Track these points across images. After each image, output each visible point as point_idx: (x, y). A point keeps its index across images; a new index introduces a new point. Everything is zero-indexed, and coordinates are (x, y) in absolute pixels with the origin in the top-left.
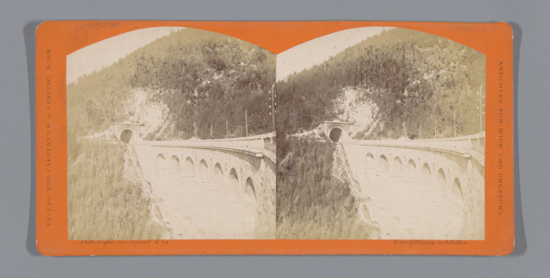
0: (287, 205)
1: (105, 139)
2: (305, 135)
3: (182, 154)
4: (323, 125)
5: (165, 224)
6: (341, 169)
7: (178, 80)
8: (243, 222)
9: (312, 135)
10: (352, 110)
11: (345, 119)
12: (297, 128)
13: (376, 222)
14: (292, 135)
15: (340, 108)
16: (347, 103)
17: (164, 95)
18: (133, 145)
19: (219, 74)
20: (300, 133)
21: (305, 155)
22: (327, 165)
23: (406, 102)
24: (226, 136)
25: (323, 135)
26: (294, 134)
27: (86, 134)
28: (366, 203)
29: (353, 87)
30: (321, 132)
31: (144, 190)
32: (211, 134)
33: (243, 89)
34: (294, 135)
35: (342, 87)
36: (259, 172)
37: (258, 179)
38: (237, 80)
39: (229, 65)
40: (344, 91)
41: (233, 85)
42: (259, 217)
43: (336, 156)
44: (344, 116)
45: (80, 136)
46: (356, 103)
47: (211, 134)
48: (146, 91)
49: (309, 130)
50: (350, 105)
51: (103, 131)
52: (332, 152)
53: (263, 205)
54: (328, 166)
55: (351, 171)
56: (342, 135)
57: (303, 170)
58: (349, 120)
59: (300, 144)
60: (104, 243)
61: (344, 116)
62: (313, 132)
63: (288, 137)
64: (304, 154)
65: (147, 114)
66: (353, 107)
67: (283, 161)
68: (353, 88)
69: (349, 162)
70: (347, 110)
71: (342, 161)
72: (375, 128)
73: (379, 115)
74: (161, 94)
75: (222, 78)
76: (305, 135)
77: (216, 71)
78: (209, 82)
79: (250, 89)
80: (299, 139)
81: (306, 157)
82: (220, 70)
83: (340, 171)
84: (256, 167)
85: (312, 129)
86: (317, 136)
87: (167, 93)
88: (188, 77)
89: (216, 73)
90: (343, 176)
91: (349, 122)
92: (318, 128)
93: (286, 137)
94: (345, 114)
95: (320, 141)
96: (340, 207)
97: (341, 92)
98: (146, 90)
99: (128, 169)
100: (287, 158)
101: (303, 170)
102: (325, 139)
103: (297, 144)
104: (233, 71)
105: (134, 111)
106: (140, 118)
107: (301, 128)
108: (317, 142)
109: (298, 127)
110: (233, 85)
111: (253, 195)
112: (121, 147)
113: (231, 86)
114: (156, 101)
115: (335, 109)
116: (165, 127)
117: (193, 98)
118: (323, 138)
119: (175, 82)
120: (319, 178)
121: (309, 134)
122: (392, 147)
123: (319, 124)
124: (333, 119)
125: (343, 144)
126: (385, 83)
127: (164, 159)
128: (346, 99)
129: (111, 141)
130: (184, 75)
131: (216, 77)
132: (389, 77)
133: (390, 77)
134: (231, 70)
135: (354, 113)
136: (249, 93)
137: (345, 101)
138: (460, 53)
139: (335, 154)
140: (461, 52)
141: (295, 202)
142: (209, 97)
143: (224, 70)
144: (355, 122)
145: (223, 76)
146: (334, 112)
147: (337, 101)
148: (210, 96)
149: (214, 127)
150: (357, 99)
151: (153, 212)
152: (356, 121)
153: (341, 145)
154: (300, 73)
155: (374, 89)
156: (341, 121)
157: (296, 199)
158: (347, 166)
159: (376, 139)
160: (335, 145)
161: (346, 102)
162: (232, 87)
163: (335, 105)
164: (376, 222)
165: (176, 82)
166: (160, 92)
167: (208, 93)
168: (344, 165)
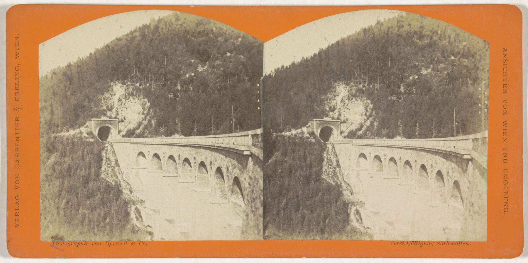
0: (273, 209)
1: (81, 136)
2: (72, 134)
3: (165, 152)
4: (91, 122)
5: (146, 227)
6: (110, 169)
7: (159, 73)
8: (230, 225)
9: (79, 134)
10: (121, 106)
11: (113, 116)
12: (285, 126)
13: (149, 226)
14: (279, 134)
15: (108, 104)
16: (116, 98)
17: (144, 89)
18: (111, 143)
19: (205, 65)
20: (288, 132)
21: (72, 155)
22: (96, 165)
23: (180, 97)
24: (211, 132)
25: (312, 134)
26: (60, 133)
27: (61, 132)
28: (139, 206)
29: (121, 81)
30: (89, 130)
31: (123, 191)
32: (195, 130)
33: (230, 82)
34: (60, 134)
35: (110, 81)
36: (247, 171)
37: (246, 179)
38: (223, 71)
39: (214, 56)
40: (112, 85)
41: (218, 78)
42: (247, 219)
43: (105, 156)
44: (113, 113)
45: (53, 133)
46: (125, 99)
47: (195, 130)
48: (125, 84)
49: (76, 129)
50: (118, 101)
51: (79, 128)
52: (100, 152)
53: (251, 207)
54: (96, 167)
55: (121, 172)
56: (111, 134)
57: (70, 171)
58: (118, 117)
59: (287, 144)
60: (77, 244)
61: (113, 113)
62: (80, 130)
63: (274, 135)
64: (70, 154)
65: (127, 109)
66: (122, 103)
67: (48, 162)
68: (122, 82)
69: (119, 162)
70: (116, 106)
71: (112, 161)
72: (146, 125)
73: (150, 111)
74: (141, 87)
75: (207, 70)
76: (72, 134)
77: (200, 63)
78: (193, 74)
79: (237, 81)
80: (65, 139)
81: (294, 157)
82: (205, 61)
83: (109, 172)
84: (244, 166)
85: (301, 127)
86: (85, 135)
87: (148, 87)
88: (170, 69)
89: (201, 64)
90: (112, 177)
91: (118, 119)
92: (85, 126)
93: (273, 136)
94: (114, 110)
95: (309, 140)
96: (111, 211)
97: (108, 87)
98: (125, 83)
99: (105, 169)
100: (274, 158)
101: (70, 171)
102: (314, 138)
103: (285, 144)
104: (219, 62)
105: (111, 106)
106: (119, 113)
107: (67, 127)
108: (306, 141)
109: (286, 124)
110: (218, 78)
111: (241, 196)
112: (99, 146)
113: (217, 79)
114: (136, 95)
115: (102, 106)
116: (145, 122)
117: (176, 92)
118: (91, 137)
119: (156, 75)
120: (308, 180)
121: (76, 133)
122: (166, 145)
123: (308, 122)
124: (101, 116)
125: (112, 143)
126: (156, 77)
127: (146, 158)
128: (114, 95)
129: (87, 138)
130: (165, 67)
131: (200, 69)
132: (160, 70)
133: (161, 70)
134: (217, 61)
135: (124, 109)
136: (235, 86)
137: (113, 96)
138: (237, 42)
139: (104, 154)
140: (237, 41)
141: (282, 206)
142: (193, 91)
143: (208, 61)
144: (125, 118)
145: (208, 67)
146: (102, 109)
147: (105, 96)
148: (193, 89)
149: (198, 123)
150: (127, 95)
151: (133, 215)
152: (126, 118)
153: (110, 144)
154: (288, 67)
155: (144, 83)
156: (110, 118)
157: (283, 202)
158: (116, 166)
159: (148, 137)
160: (103, 144)
161: (114, 97)
162: (217, 80)
163: (103, 102)
164: (149, 226)
165: (157, 75)
166: (140, 85)
167: (191, 86)
168: (113, 165)
